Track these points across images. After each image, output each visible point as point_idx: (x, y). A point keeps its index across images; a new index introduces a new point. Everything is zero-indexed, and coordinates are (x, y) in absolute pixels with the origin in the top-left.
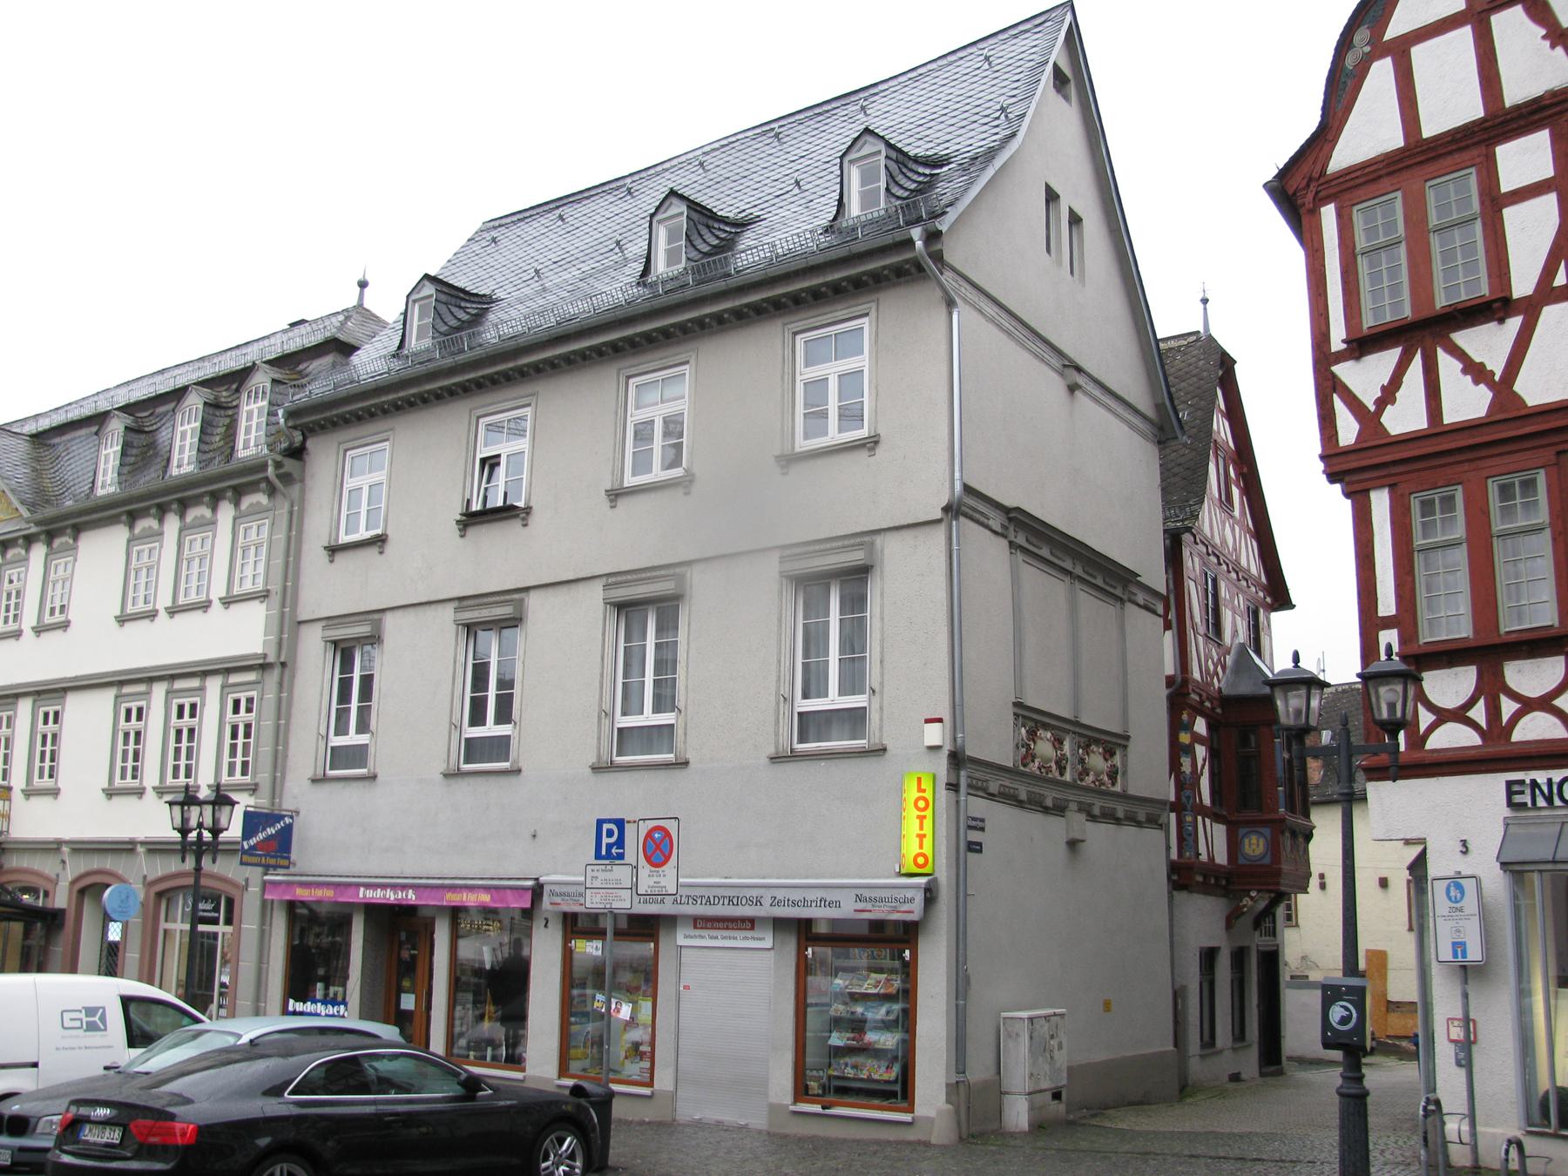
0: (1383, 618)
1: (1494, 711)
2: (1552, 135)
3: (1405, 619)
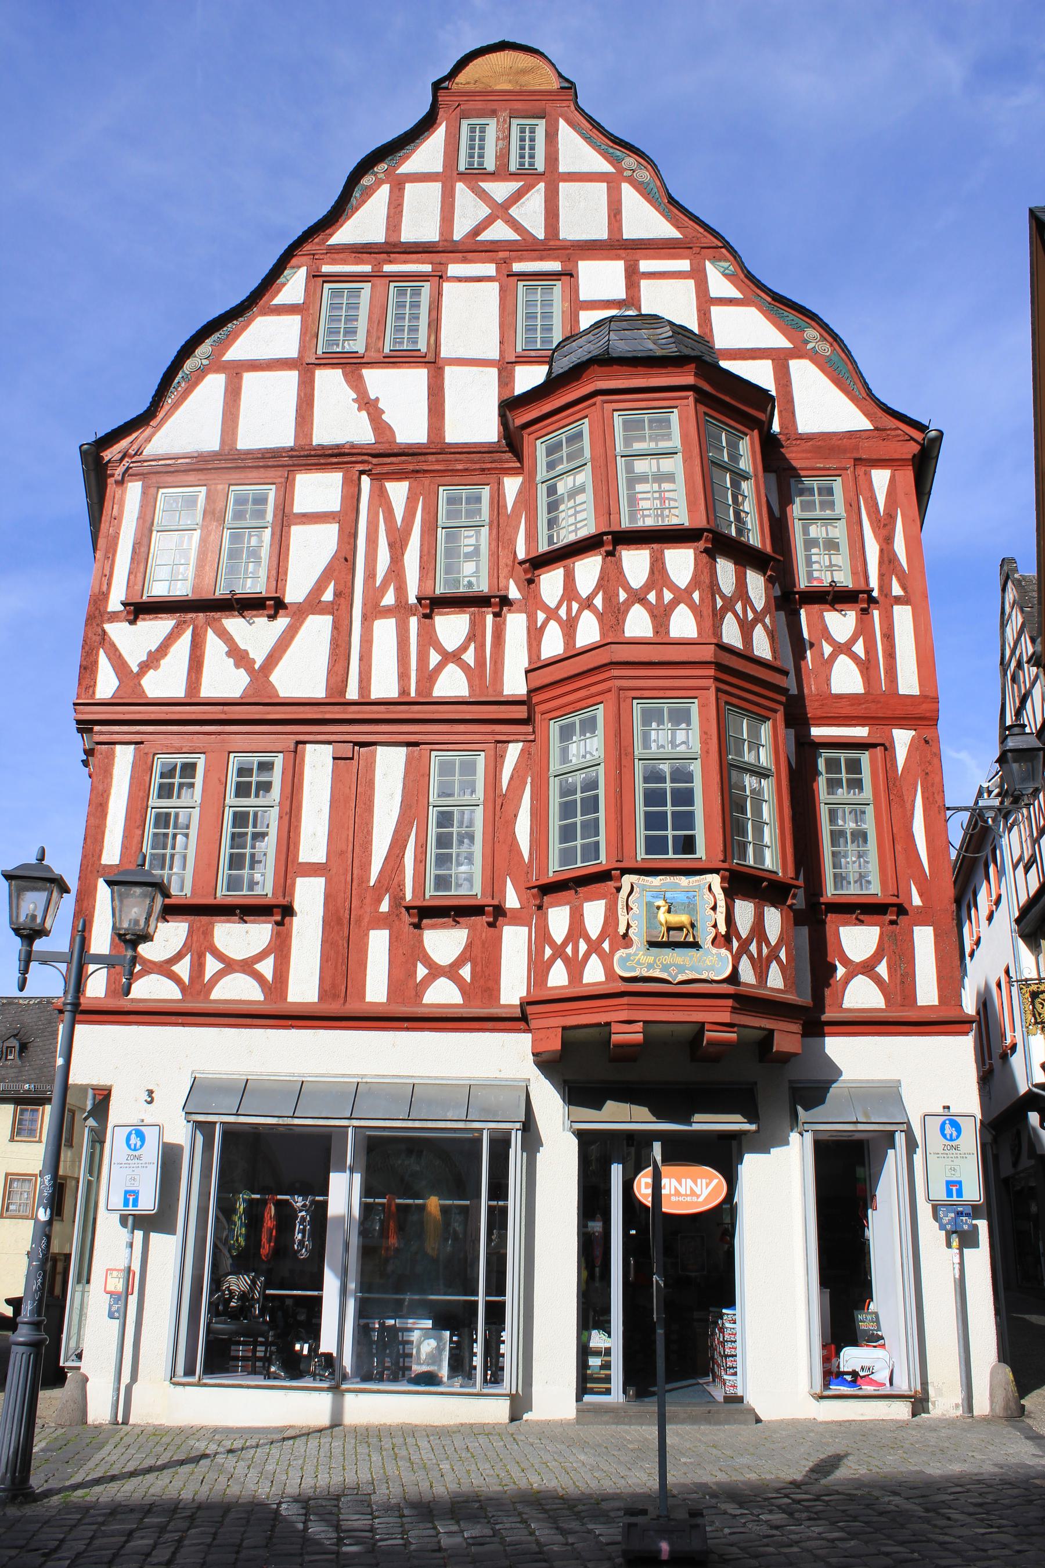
1: (198, 968)
2: (344, 479)
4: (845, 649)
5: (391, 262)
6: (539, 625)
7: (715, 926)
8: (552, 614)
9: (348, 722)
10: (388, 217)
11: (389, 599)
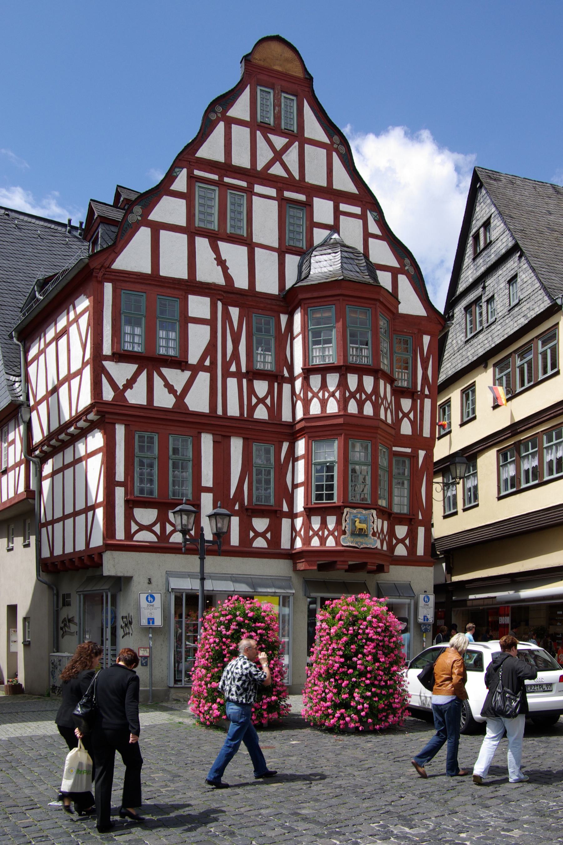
0: (118, 482)
4: (406, 415)
5: (227, 177)
11: (233, 368)
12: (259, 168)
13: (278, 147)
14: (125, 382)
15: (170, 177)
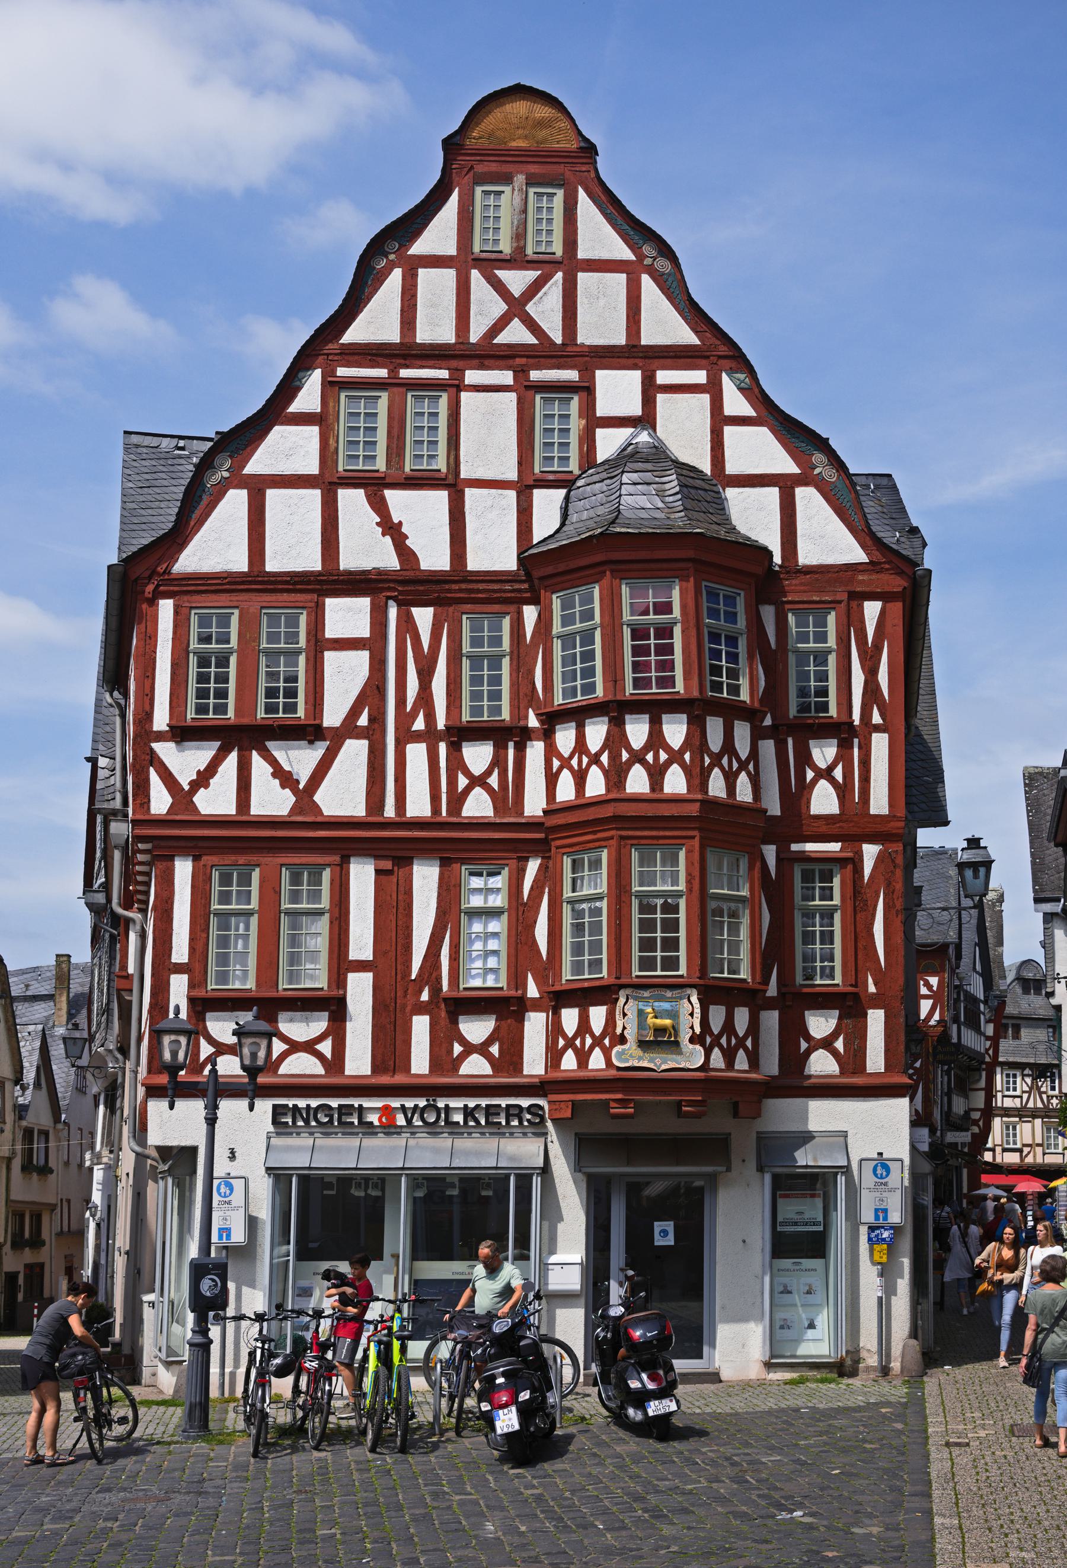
2: (372, 604)
3: (196, 968)
5: (407, 367)
6: (554, 770)
7: (692, 1028)
8: (565, 763)
9: (392, 844)
10: (402, 310)
11: (419, 724)
12: (474, 338)
13: (516, 290)
14: (195, 777)
15: (288, 387)
